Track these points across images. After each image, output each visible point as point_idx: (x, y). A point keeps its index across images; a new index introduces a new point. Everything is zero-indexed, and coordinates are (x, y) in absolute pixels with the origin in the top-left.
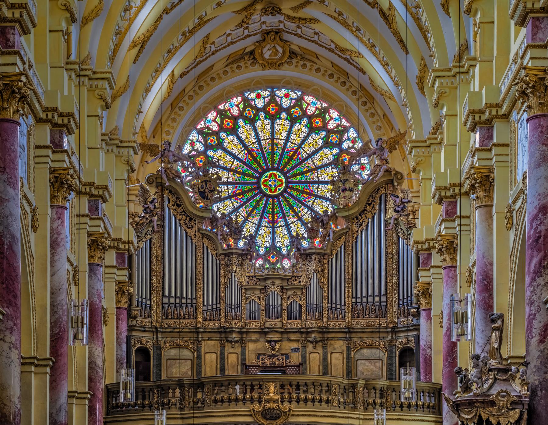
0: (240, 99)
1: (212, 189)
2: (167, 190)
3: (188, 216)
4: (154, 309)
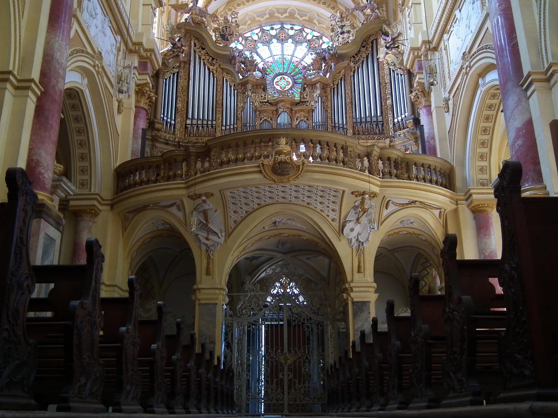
0: (259, 30)
1: (231, 33)
2: (194, 37)
3: (211, 57)
4: (178, 126)
